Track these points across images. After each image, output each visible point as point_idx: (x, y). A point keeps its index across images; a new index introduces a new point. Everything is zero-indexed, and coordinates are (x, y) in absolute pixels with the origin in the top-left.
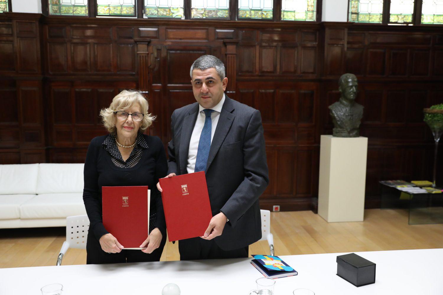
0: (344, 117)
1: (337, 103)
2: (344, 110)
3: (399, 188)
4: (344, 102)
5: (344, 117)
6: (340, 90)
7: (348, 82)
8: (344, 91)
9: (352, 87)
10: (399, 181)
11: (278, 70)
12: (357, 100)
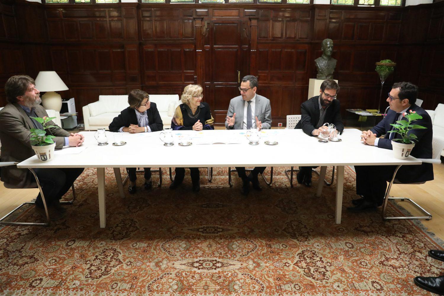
0: (324, 67)
1: (320, 58)
2: (324, 62)
3: (357, 113)
4: (324, 57)
5: (324, 67)
6: (322, 50)
7: (327, 44)
8: (324, 50)
9: (329, 47)
10: (358, 109)
11: (284, 36)
12: (333, 55)
